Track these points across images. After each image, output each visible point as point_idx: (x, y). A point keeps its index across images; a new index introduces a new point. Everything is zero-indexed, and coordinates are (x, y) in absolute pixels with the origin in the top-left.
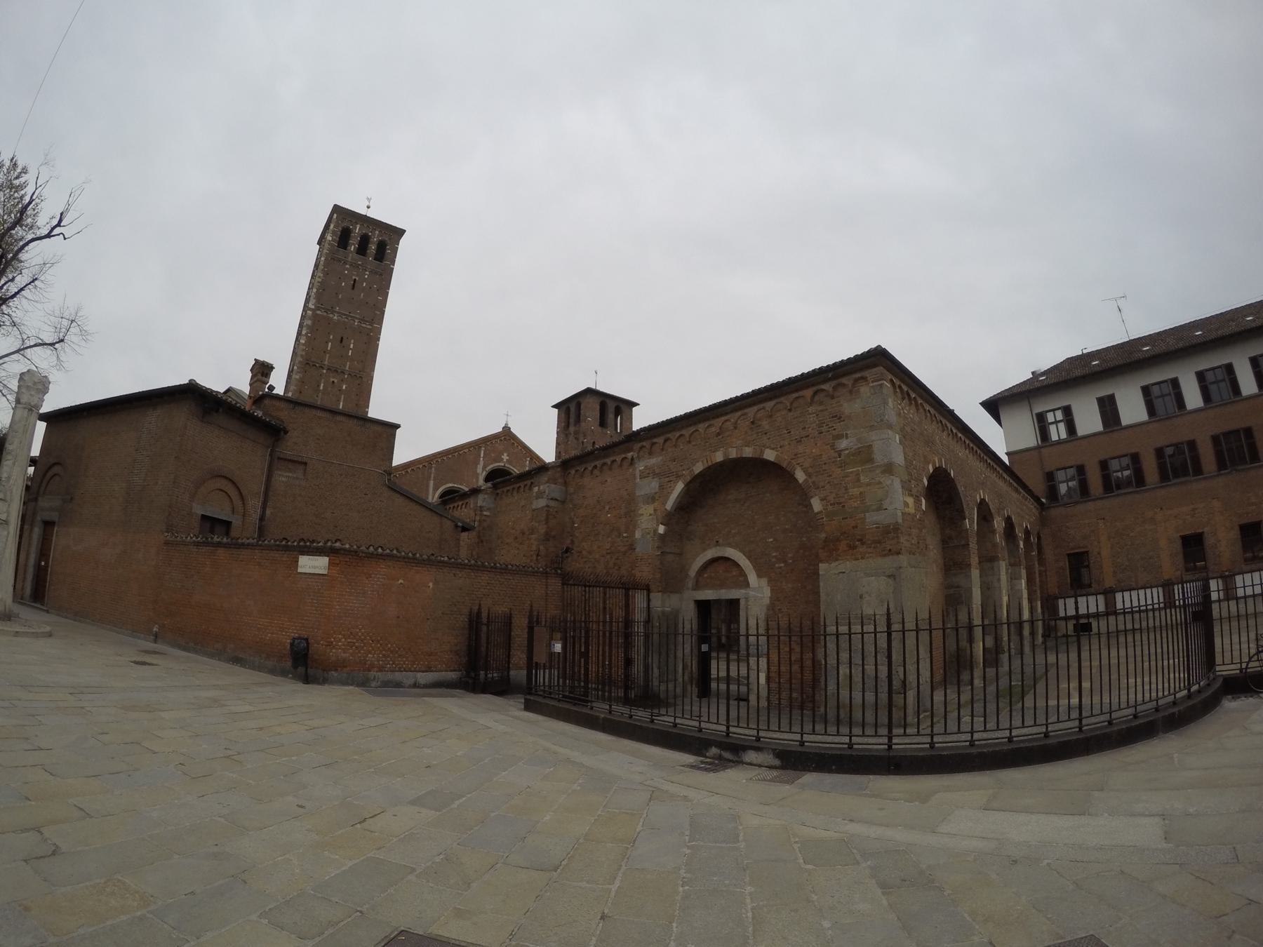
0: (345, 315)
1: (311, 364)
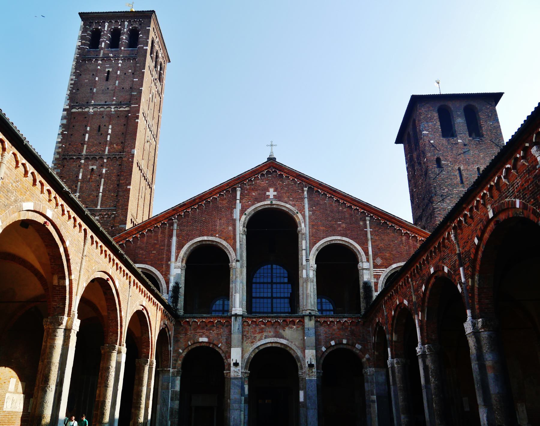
0: (99, 105)
1: (68, 157)
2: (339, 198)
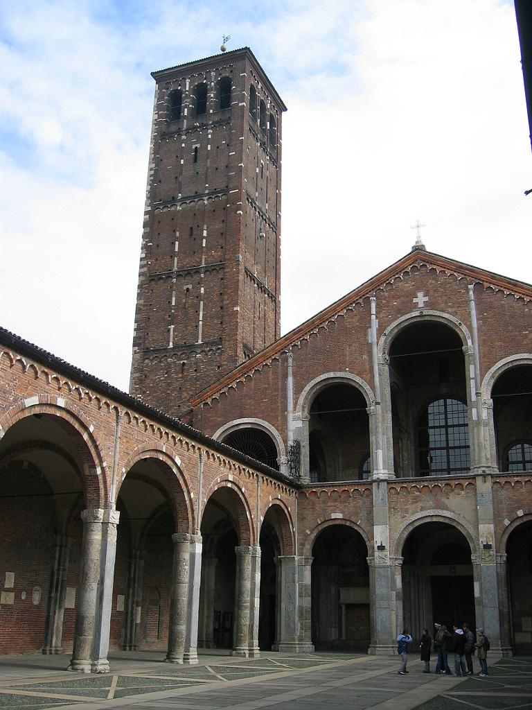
0: (188, 198)
2: (523, 294)
